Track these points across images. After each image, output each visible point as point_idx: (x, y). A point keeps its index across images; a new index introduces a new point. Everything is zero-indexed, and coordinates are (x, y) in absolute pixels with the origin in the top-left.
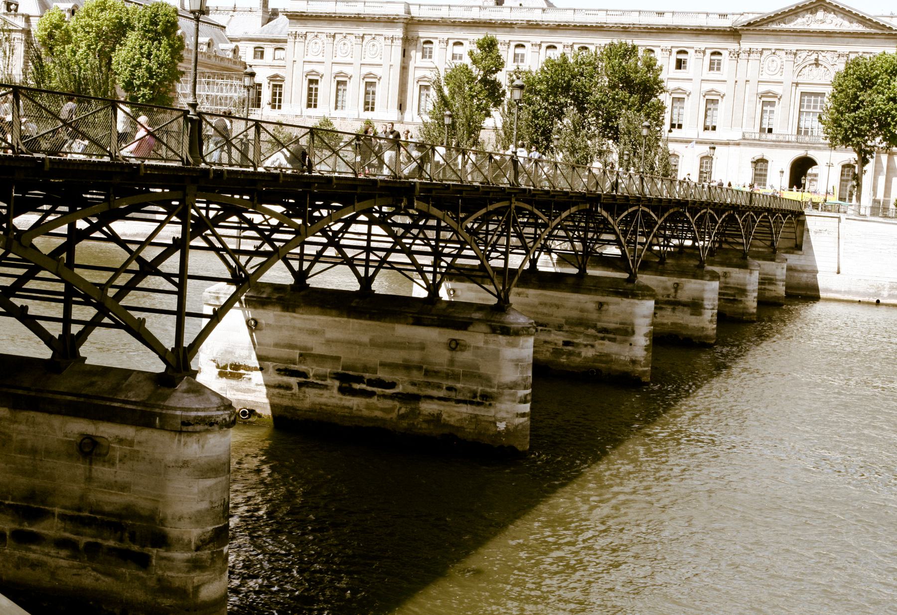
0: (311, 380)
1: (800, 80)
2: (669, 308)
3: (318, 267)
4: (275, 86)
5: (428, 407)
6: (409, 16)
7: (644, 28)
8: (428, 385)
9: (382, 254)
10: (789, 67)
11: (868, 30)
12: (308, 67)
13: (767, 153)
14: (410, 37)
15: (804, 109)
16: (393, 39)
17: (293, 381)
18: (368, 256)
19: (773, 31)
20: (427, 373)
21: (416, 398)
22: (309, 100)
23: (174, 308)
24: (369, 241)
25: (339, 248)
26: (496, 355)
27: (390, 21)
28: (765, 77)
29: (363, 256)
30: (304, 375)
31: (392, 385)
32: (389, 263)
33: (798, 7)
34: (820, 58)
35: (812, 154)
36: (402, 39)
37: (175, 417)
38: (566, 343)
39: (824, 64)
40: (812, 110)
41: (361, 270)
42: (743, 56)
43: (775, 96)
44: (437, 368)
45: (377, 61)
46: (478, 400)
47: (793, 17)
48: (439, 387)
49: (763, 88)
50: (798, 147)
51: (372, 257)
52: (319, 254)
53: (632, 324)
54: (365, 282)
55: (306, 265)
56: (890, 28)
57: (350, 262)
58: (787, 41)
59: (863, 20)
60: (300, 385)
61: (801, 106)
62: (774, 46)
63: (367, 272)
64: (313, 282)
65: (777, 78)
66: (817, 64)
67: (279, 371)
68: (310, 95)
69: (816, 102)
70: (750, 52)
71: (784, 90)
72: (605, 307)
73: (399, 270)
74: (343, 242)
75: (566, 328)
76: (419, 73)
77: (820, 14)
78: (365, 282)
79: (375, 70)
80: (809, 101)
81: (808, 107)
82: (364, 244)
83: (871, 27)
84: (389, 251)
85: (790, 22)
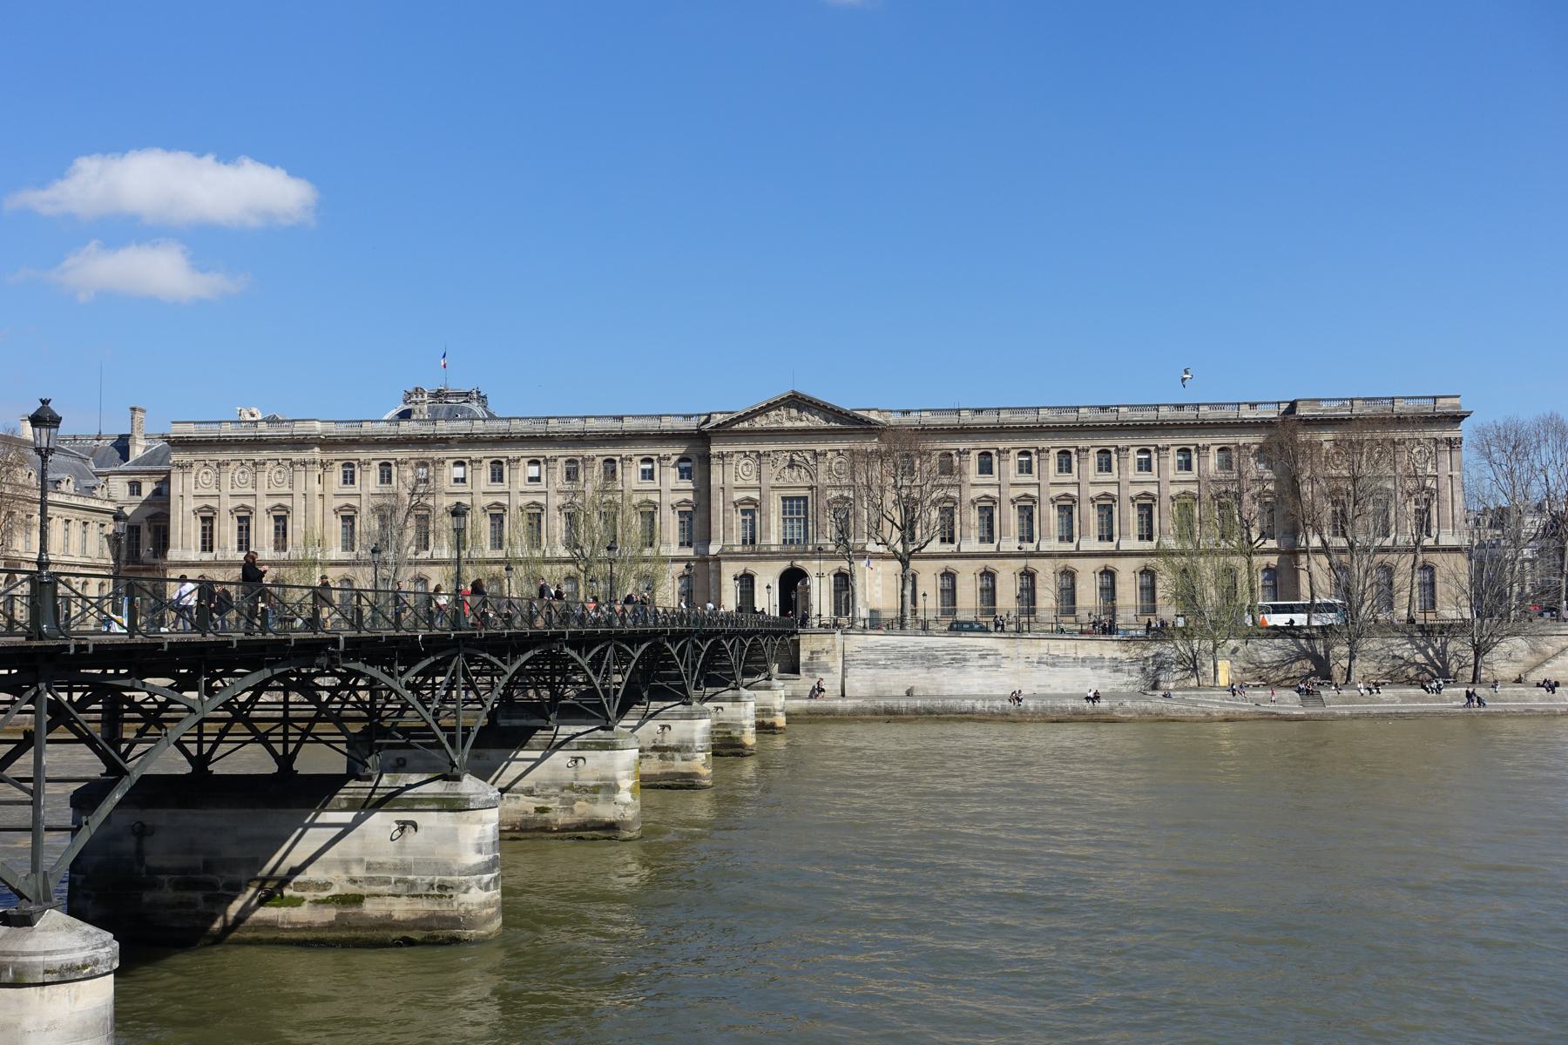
0: (221, 891)
1: (781, 483)
2: (656, 755)
3: (223, 748)
4: (157, 529)
5: (371, 908)
8: (371, 881)
9: (304, 725)
12: (201, 503)
13: (752, 567)
17: (198, 896)
18: (286, 729)
20: (369, 867)
21: (358, 900)
22: (204, 542)
23: (29, 823)
24: (286, 710)
25: (249, 722)
26: (453, 837)
28: (740, 483)
29: (280, 730)
30: (212, 885)
31: (326, 886)
32: (314, 735)
34: (796, 457)
35: (799, 563)
37: (33, 965)
38: (537, 810)
41: (279, 748)
42: (713, 460)
43: (750, 501)
44: (380, 859)
45: (286, 490)
46: (436, 892)
48: (387, 882)
49: (738, 496)
50: (785, 558)
51: (291, 730)
52: (223, 733)
53: (614, 779)
54: (286, 761)
55: (206, 748)
56: (869, 422)
57: (262, 739)
58: (762, 442)
60: (206, 899)
62: (747, 448)
63: (285, 749)
64: (216, 769)
65: (754, 482)
67: (177, 886)
68: (204, 536)
70: (722, 456)
72: (581, 762)
73: (328, 743)
74: (254, 714)
75: (537, 791)
78: (286, 761)
79: (286, 502)
81: (791, 513)
82: (280, 714)
83: (849, 422)
84: (312, 721)
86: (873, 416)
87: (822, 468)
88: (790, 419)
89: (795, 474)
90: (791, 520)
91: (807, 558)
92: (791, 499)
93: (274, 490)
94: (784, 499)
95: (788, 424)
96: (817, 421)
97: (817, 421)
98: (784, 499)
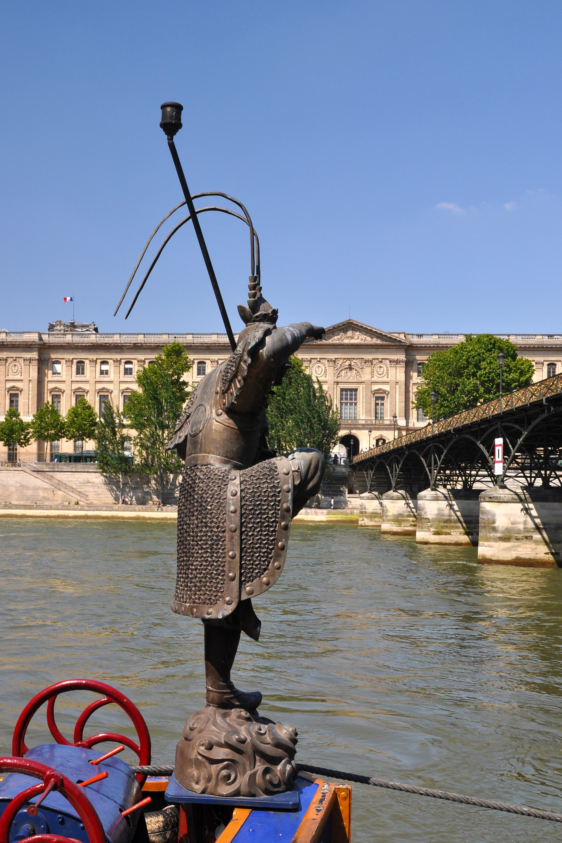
1: (339, 380)
6: (41, 342)
7: (222, 346)
10: (330, 371)
11: (385, 343)
14: (42, 359)
15: (344, 401)
16: (30, 360)
19: (318, 345)
27: (27, 347)
33: (334, 328)
34: (353, 363)
36: (38, 360)
39: (356, 368)
40: (349, 401)
45: (18, 377)
47: (331, 335)
59: (379, 336)
61: (341, 399)
62: (318, 356)
66: (350, 368)
69: (351, 395)
71: (329, 388)
76: (51, 386)
77: (350, 333)
80: (346, 395)
81: (346, 399)
83: (386, 341)
85: (330, 338)
86: (402, 336)
87: (368, 370)
88: (347, 338)
89: (349, 374)
90: (346, 404)
91: (359, 429)
92: (347, 390)
93: (10, 377)
94: (342, 390)
95: (346, 341)
96: (369, 340)
97: (369, 340)
98: (342, 390)
